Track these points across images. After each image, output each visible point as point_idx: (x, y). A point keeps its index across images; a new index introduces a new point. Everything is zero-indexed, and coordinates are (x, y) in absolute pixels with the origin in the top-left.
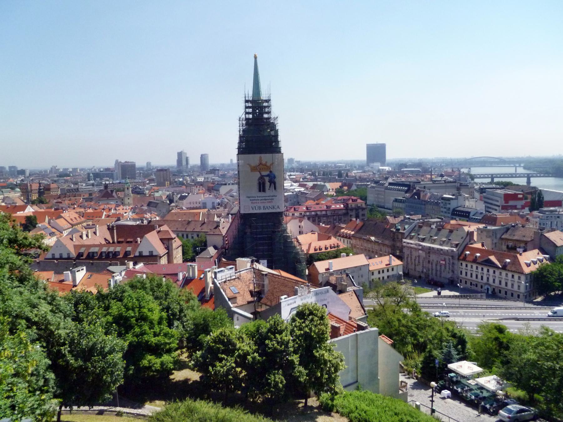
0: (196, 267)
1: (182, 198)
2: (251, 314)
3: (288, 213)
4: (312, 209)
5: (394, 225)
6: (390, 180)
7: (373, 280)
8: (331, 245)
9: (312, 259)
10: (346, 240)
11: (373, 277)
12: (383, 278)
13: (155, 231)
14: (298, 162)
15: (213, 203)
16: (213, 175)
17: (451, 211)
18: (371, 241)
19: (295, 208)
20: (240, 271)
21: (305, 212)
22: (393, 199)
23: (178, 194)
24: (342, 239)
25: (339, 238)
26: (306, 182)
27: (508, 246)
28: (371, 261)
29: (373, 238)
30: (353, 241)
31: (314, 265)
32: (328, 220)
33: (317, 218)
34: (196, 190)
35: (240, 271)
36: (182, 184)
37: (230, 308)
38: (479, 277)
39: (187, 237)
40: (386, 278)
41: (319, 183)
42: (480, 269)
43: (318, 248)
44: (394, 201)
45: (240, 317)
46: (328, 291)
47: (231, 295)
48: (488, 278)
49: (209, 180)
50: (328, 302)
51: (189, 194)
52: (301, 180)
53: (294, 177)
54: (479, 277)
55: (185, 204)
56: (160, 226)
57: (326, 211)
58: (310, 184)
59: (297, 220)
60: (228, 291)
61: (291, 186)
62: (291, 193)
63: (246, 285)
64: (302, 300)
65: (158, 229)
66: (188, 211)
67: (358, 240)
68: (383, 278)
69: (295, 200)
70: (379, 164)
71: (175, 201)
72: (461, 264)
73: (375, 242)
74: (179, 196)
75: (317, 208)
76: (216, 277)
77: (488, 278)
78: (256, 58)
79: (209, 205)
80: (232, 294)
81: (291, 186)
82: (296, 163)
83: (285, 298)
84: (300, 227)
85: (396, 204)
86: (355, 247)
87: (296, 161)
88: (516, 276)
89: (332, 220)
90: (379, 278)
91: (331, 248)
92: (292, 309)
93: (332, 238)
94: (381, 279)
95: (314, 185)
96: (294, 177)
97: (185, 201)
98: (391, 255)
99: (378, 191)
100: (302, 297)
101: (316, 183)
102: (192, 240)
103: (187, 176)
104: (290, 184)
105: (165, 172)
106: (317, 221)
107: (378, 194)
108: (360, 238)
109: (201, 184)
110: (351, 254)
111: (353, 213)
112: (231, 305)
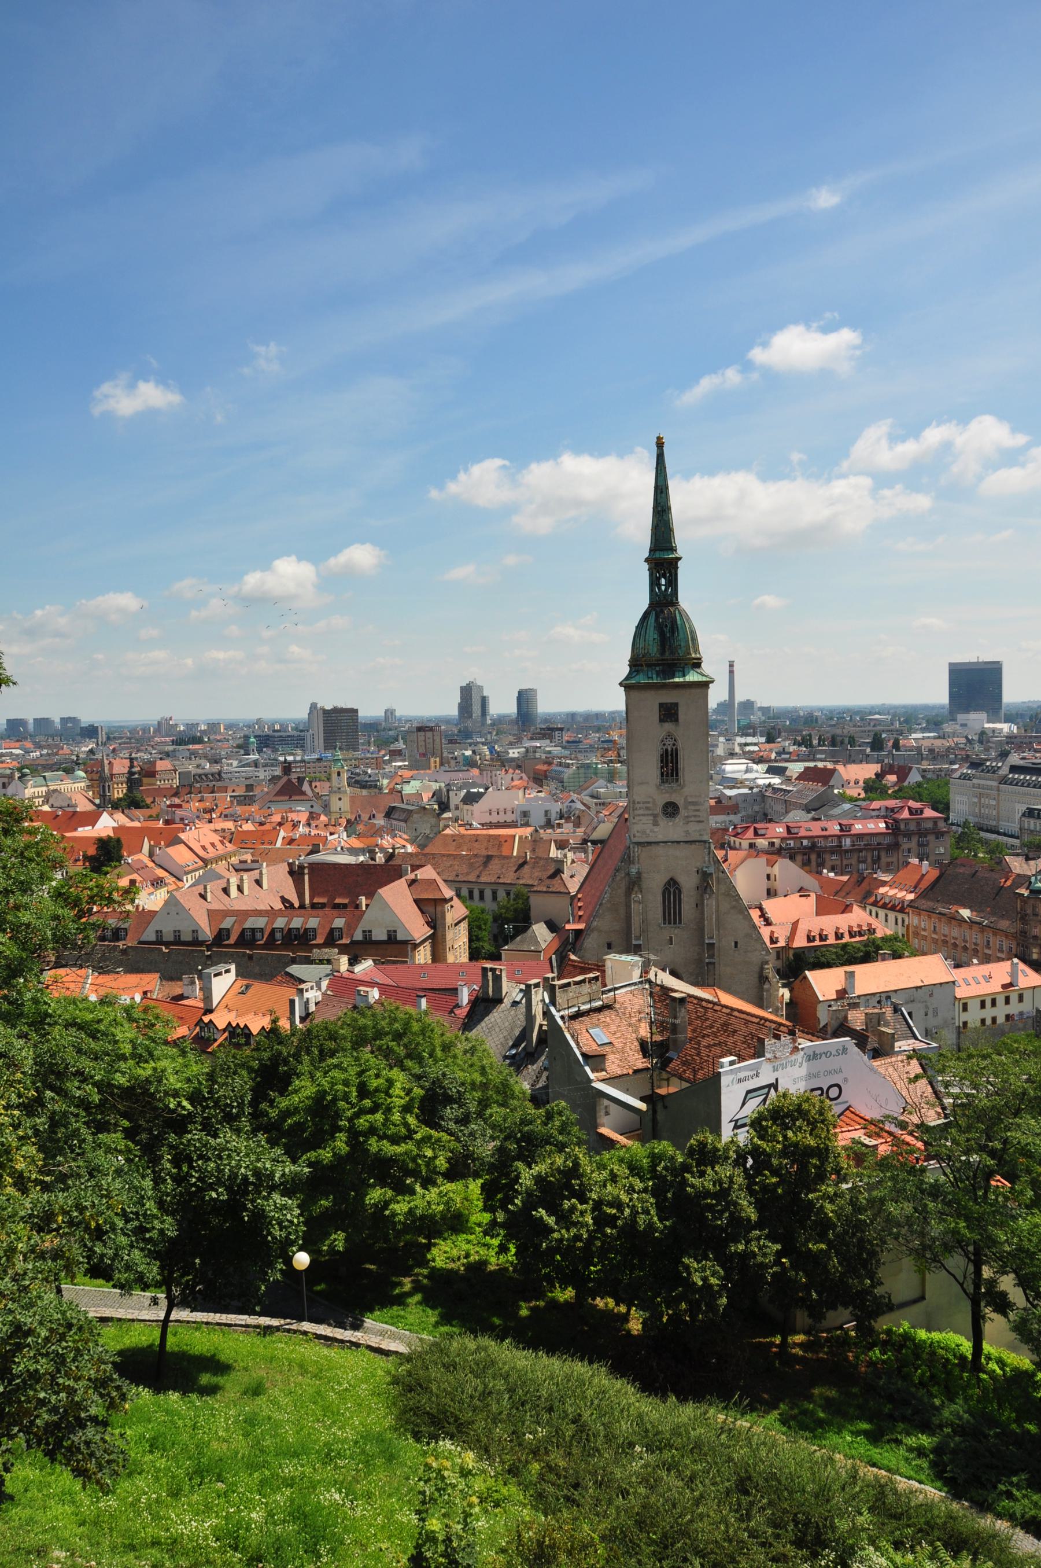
0: (504, 975)
1: (471, 799)
2: (642, 1099)
3: (738, 840)
4: (803, 833)
5: (1024, 880)
6: (1015, 759)
7: (965, 1024)
8: (850, 927)
9: (796, 964)
10: (892, 916)
11: (964, 1017)
12: (994, 1020)
13: (403, 879)
14: (765, 710)
16: (548, 741)
18: (963, 920)
19: (755, 828)
20: (616, 989)
21: (783, 839)
22: (1023, 808)
23: (460, 789)
24: (882, 913)
25: (874, 909)
26: (787, 761)
28: (958, 974)
29: (966, 913)
30: (913, 920)
31: (805, 977)
32: (845, 862)
33: (813, 857)
34: (504, 777)
35: (616, 989)
36: (470, 763)
37: (590, 1081)
39: (482, 897)
40: (1001, 1020)
41: (820, 765)
43: (815, 933)
44: (1024, 815)
45: (614, 1108)
46: (845, 1050)
47: (591, 1048)
49: (538, 755)
50: (845, 1080)
51: (487, 789)
52: (773, 756)
53: (756, 748)
55: (477, 814)
56: (415, 868)
57: (839, 837)
58: (796, 768)
60: (582, 1041)
61: (747, 771)
62: (746, 791)
63: (630, 1025)
64: (775, 1070)
65: (412, 876)
66: (485, 832)
67: (924, 916)
68: (994, 1020)
69: (756, 808)
70: (983, 716)
71: (452, 806)
73: (972, 922)
75: (816, 829)
76: (553, 1002)
79: (537, 818)
80: (594, 1047)
81: (747, 771)
82: (760, 713)
83: (732, 1063)
84: (768, 877)
86: (916, 934)
87: (761, 709)
89: (854, 861)
90: (983, 1021)
91: (851, 936)
92: (748, 1092)
93: (855, 907)
94: (988, 1022)
95: (807, 769)
96: (756, 748)
97: (477, 807)
98: (1016, 960)
99: (979, 786)
101: (811, 764)
102: (494, 907)
103: (483, 744)
104: (744, 767)
105: (429, 734)
106: (814, 864)
107: (980, 796)
108: (931, 911)
109: (518, 765)
112: (592, 1076)
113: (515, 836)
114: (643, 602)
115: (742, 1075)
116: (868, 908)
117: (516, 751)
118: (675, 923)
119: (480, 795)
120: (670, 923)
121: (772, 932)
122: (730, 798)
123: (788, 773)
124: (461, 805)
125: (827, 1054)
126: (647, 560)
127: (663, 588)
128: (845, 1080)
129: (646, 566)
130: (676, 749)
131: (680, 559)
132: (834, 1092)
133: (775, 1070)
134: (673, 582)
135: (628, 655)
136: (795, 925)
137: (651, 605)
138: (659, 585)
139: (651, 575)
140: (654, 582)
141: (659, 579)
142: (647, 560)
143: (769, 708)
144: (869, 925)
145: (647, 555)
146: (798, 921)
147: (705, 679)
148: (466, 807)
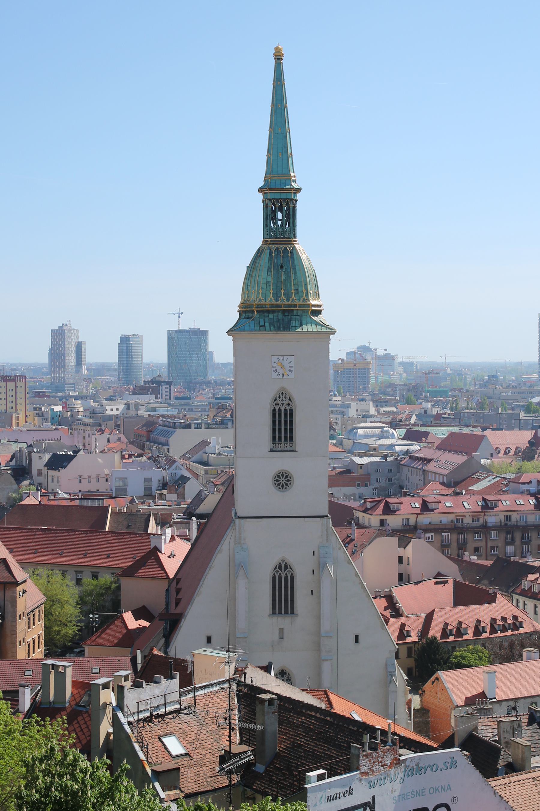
1: (58, 462)
8: (494, 620)
14: (407, 366)
15: (148, 480)
16: (153, 397)
23: (45, 451)
24: (531, 603)
25: (522, 599)
32: (490, 544)
41: (466, 430)
46: (454, 763)
49: (140, 413)
50: (455, 799)
51: (76, 452)
52: (413, 419)
58: (440, 433)
59: (395, 539)
62: (377, 459)
71: (34, 472)
74: (47, 457)
78: (278, 57)
79: (136, 488)
82: (401, 369)
83: (320, 778)
84: (400, 560)
87: (401, 364)
93: (499, 597)
100: (372, 778)
101: (456, 429)
105: (11, 385)
109: (118, 423)
113: (107, 509)
114: (256, 239)
115: (332, 792)
116: (516, 597)
117: (115, 408)
118: (286, 613)
119: (68, 459)
120: (280, 613)
121: (403, 626)
122: (361, 466)
123: (430, 439)
125: (434, 768)
126: (261, 190)
127: (279, 223)
128: (455, 799)
129: (260, 197)
130: (291, 410)
131: (298, 190)
133: (371, 785)
134: (291, 216)
135: (237, 299)
136: (429, 617)
137: (265, 242)
138: (275, 219)
140: (269, 216)
141: (274, 212)
142: (261, 190)
143: (411, 364)
144: (515, 618)
145: (262, 184)
146: (433, 611)
147: (324, 329)
148: (51, 473)
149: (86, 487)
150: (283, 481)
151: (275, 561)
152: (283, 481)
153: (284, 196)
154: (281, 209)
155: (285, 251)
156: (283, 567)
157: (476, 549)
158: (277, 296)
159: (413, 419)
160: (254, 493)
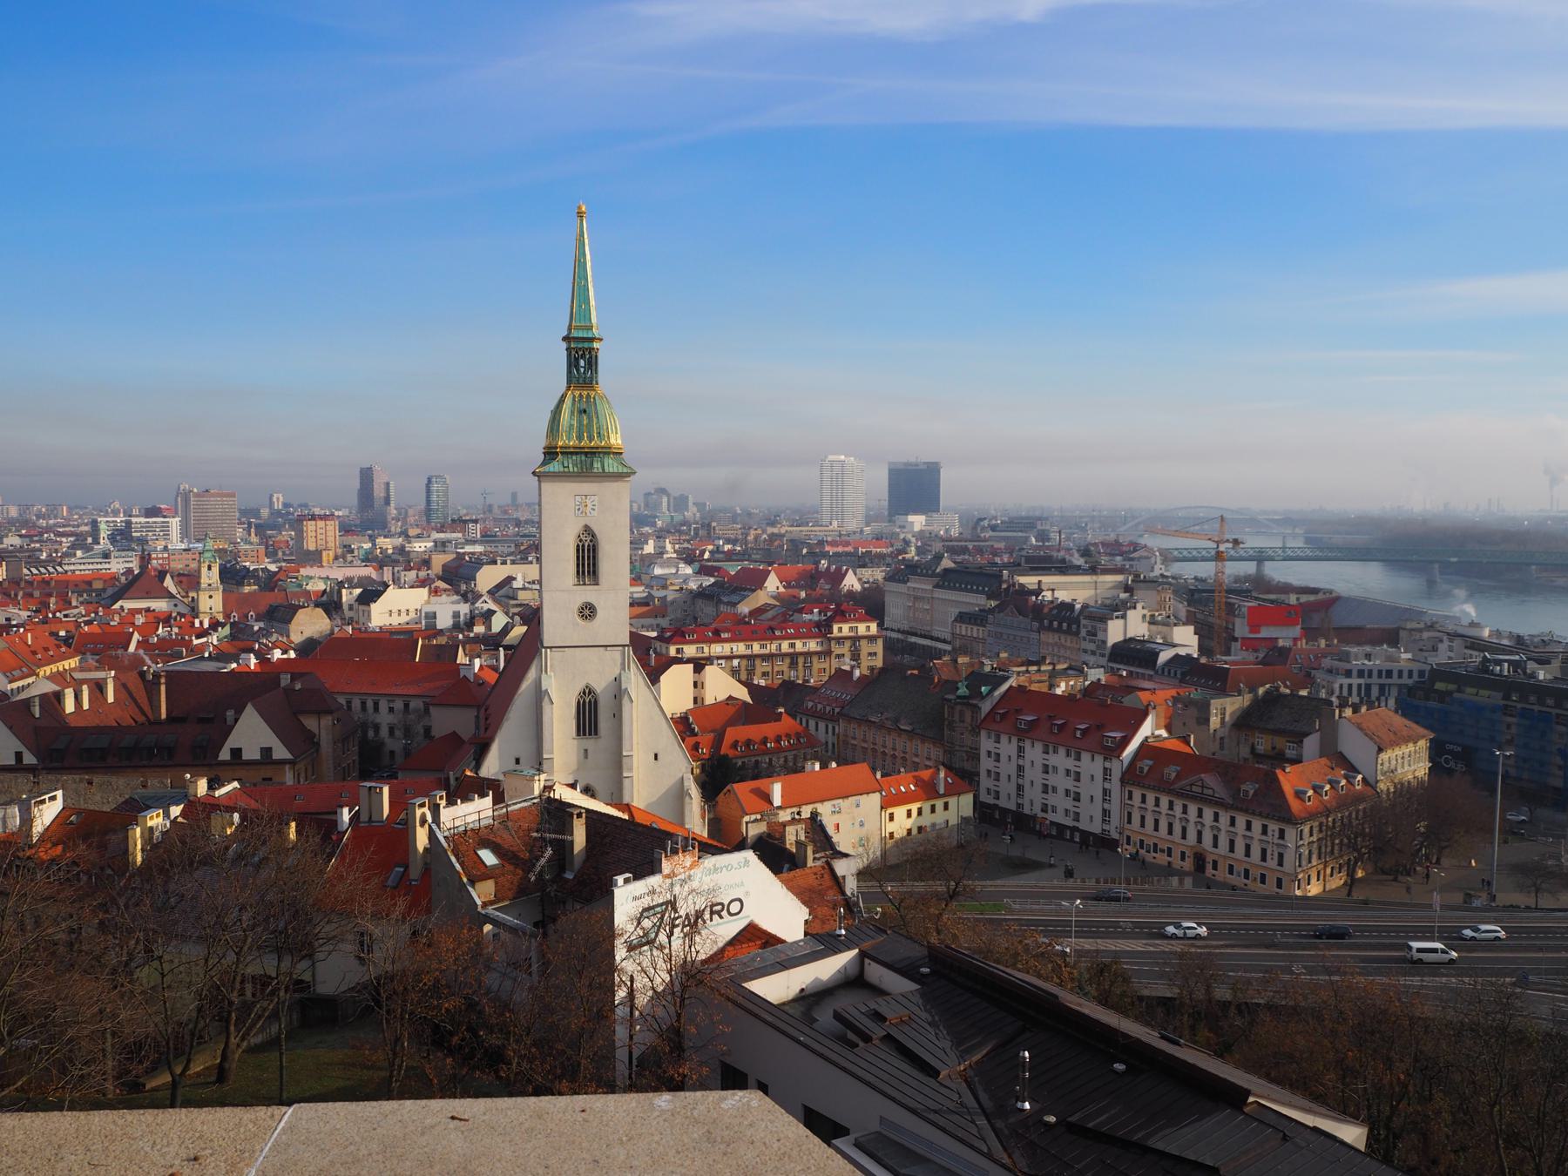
7: (891, 834)
11: (891, 827)
15: (456, 615)
17: (1107, 652)
22: (954, 611)
27: (1253, 748)
38: (1177, 829)
42: (1178, 809)
46: (747, 862)
48: (1200, 833)
50: (747, 893)
54: (1177, 829)
59: (691, 666)
72: (1130, 793)
77: (1200, 833)
85: (964, 629)
86: (846, 743)
88: (1273, 827)
92: (645, 910)
105: (321, 524)
110: (834, 765)
111: (845, 649)
124: (356, 606)
126: (564, 339)
128: (747, 893)
129: (564, 345)
132: (735, 907)
134: (592, 363)
138: (577, 366)
139: (569, 355)
140: (572, 363)
145: (565, 333)
148: (362, 607)
149: (396, 621)
150: (588, 611)
151: (579, 687)
152: (588, 611)
153: (586, 345)
154: (583, 357)
155: (588, 396)
156: (588, 691)
157: (764, 674)
158: (580, 438)
159: (706, 556)
160: (558, 625)
